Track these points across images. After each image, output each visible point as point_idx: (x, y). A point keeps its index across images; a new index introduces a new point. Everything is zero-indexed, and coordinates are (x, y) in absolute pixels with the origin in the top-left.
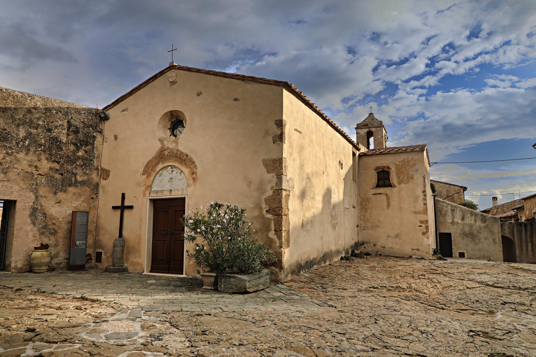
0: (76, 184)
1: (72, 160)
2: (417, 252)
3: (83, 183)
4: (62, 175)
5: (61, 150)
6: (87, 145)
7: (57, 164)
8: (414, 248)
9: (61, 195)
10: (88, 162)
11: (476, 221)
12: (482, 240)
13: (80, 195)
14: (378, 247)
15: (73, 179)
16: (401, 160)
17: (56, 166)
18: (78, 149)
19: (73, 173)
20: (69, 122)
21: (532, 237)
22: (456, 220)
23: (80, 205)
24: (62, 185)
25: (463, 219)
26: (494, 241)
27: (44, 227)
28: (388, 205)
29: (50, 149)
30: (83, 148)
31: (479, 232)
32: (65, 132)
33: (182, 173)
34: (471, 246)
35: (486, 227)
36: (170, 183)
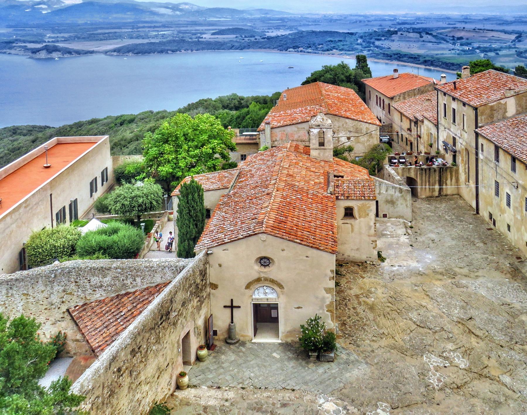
11: (395, 192)
12: (399, 205)
21: (429, 178)
22: (382, 192)
25: (387, 191)
26: (407, 206)
28: (352, 231)
31: (397, 200)
34: (391, 209)
35: (402, 196)
36: (264, 295)
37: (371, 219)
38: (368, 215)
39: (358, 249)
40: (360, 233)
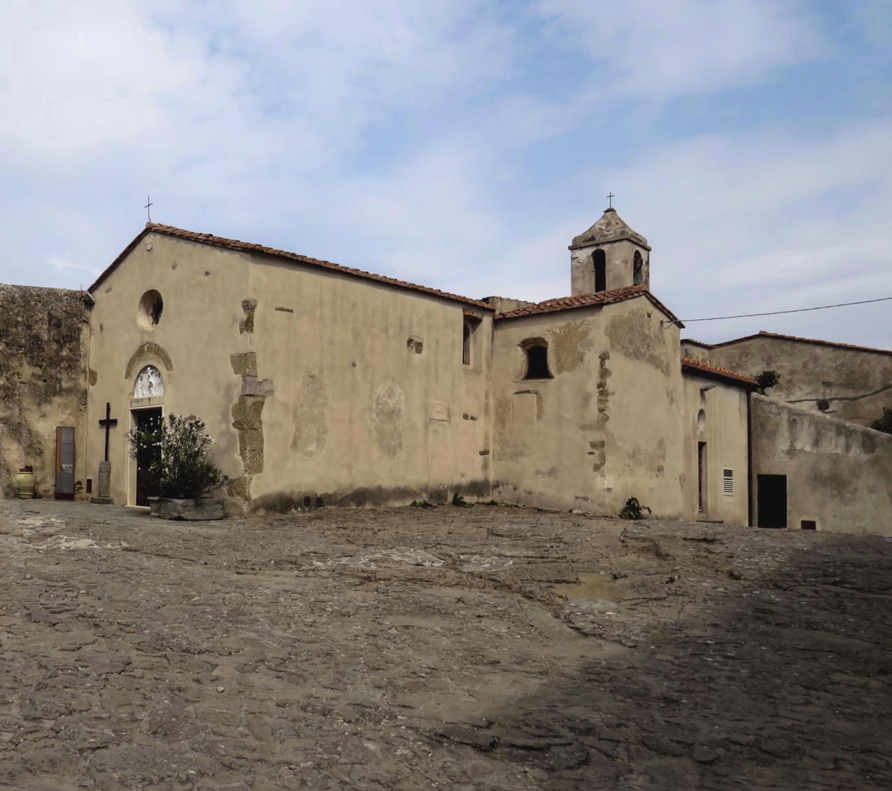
0: (60, 392)
1: (54, 362)
2: (584, 503)
3: (69, 391)
4: (45, 381)
5: (43, 350)
6: (71, 341)
8: (580, 494)
9: (46, 408)
10: (73, 364)
13: (66, 406)
14: (521, 491)
15: (58, 386)
17: (38, 371)
18: (61, 347)
19: (57, 379)
20: (49, 314)
23: (67, 419)
24: (46, 394)
27: (30, 446)
29: (31, 350)
30: (68, 345)
32: (45, 327)
37: (589, 372)
38: (581, 360)
39: (552, 472)
40: (560, 420)
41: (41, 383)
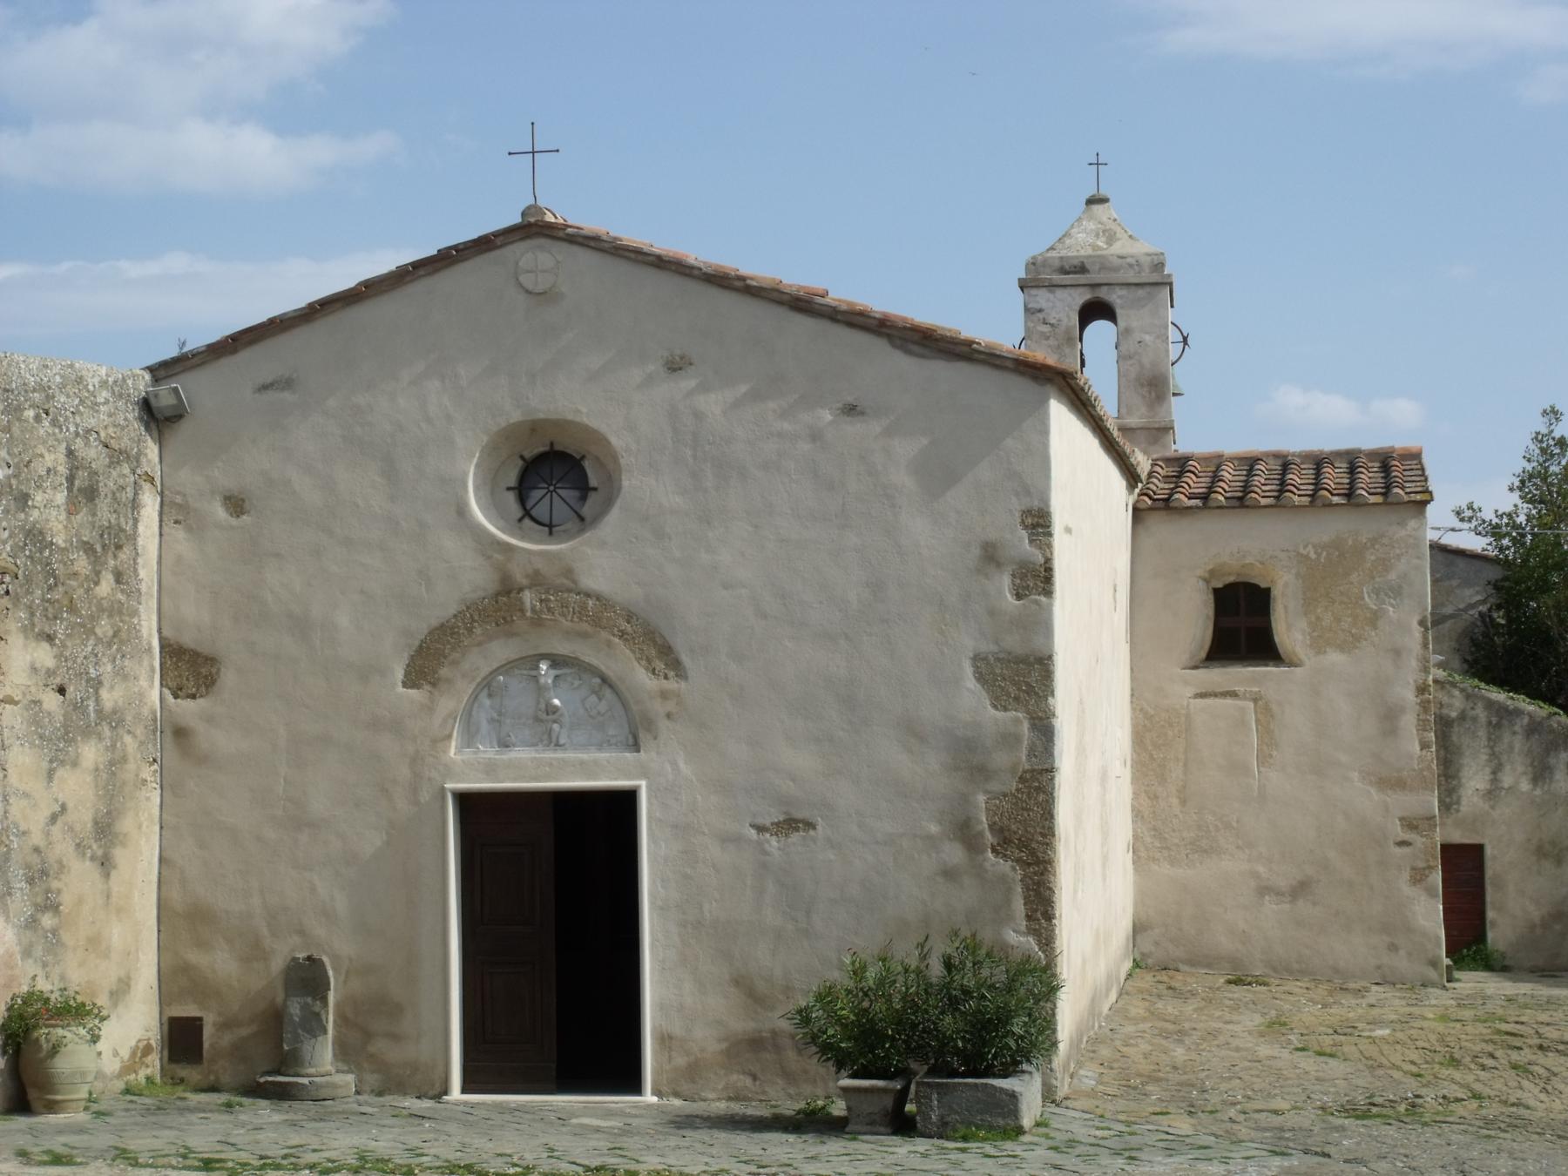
4: (62, 691)
7: (45, 645)
16: (1326, 539)
20: (70, 453)
32: (61, 497)
33: (608, 693)
41: (51, 701)
